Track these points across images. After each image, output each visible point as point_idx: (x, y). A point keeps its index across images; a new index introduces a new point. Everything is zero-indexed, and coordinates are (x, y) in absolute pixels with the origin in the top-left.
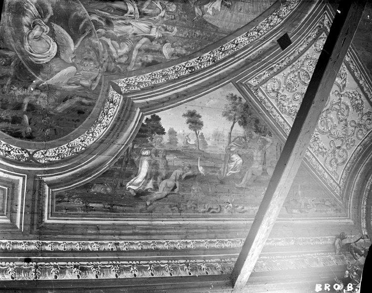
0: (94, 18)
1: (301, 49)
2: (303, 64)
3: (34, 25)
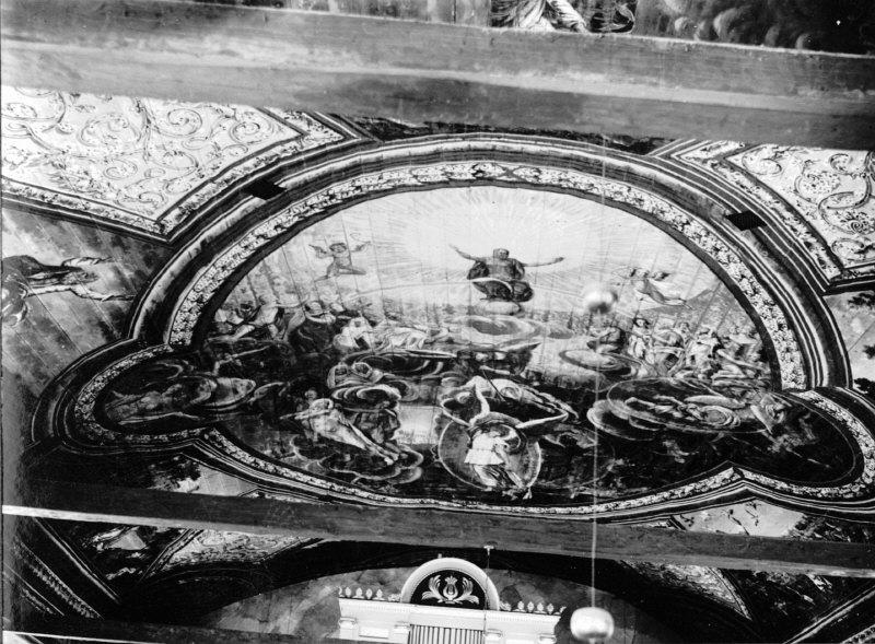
1: (768, 197)
2: (809, 200)
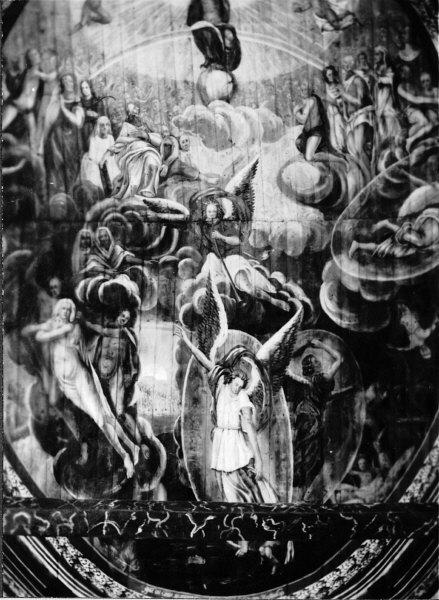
0: (382, 165)
3: (403, 241)
